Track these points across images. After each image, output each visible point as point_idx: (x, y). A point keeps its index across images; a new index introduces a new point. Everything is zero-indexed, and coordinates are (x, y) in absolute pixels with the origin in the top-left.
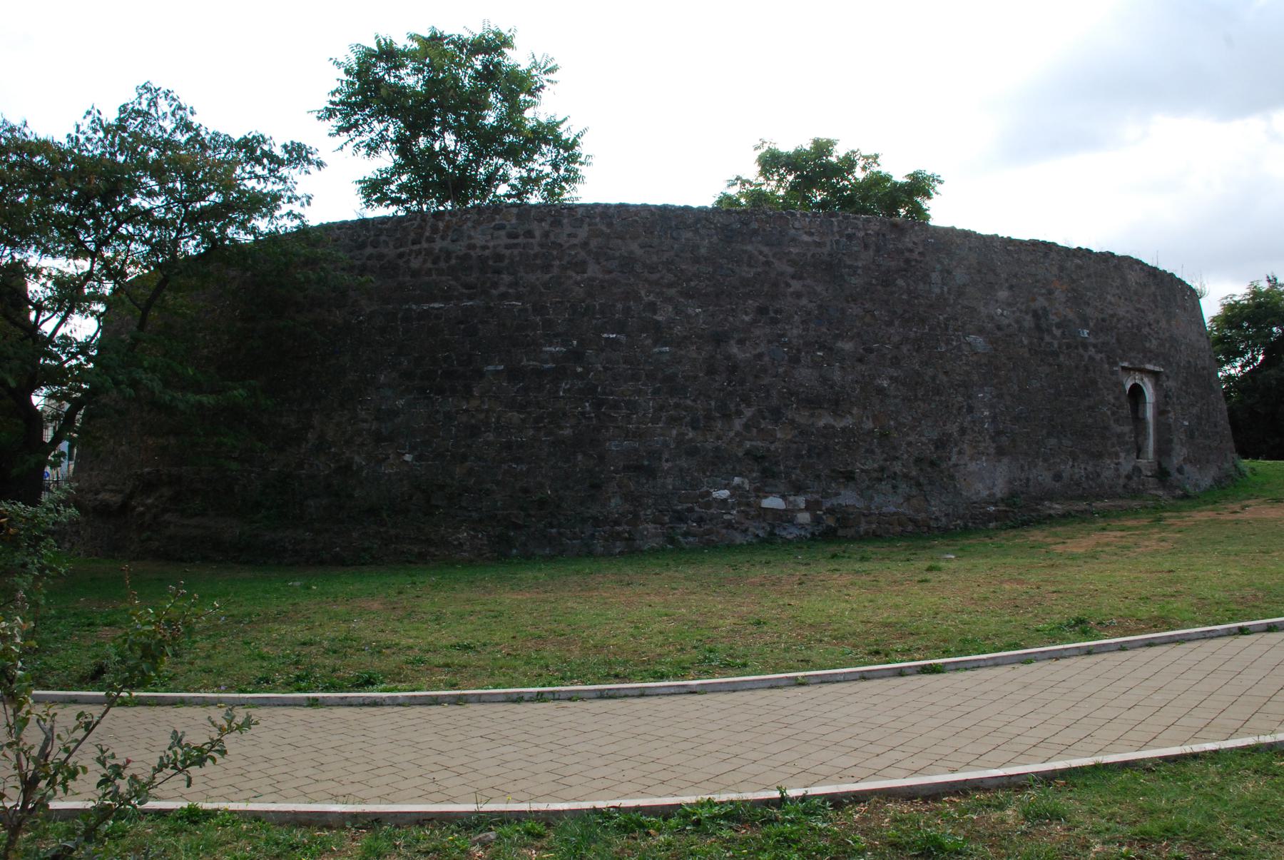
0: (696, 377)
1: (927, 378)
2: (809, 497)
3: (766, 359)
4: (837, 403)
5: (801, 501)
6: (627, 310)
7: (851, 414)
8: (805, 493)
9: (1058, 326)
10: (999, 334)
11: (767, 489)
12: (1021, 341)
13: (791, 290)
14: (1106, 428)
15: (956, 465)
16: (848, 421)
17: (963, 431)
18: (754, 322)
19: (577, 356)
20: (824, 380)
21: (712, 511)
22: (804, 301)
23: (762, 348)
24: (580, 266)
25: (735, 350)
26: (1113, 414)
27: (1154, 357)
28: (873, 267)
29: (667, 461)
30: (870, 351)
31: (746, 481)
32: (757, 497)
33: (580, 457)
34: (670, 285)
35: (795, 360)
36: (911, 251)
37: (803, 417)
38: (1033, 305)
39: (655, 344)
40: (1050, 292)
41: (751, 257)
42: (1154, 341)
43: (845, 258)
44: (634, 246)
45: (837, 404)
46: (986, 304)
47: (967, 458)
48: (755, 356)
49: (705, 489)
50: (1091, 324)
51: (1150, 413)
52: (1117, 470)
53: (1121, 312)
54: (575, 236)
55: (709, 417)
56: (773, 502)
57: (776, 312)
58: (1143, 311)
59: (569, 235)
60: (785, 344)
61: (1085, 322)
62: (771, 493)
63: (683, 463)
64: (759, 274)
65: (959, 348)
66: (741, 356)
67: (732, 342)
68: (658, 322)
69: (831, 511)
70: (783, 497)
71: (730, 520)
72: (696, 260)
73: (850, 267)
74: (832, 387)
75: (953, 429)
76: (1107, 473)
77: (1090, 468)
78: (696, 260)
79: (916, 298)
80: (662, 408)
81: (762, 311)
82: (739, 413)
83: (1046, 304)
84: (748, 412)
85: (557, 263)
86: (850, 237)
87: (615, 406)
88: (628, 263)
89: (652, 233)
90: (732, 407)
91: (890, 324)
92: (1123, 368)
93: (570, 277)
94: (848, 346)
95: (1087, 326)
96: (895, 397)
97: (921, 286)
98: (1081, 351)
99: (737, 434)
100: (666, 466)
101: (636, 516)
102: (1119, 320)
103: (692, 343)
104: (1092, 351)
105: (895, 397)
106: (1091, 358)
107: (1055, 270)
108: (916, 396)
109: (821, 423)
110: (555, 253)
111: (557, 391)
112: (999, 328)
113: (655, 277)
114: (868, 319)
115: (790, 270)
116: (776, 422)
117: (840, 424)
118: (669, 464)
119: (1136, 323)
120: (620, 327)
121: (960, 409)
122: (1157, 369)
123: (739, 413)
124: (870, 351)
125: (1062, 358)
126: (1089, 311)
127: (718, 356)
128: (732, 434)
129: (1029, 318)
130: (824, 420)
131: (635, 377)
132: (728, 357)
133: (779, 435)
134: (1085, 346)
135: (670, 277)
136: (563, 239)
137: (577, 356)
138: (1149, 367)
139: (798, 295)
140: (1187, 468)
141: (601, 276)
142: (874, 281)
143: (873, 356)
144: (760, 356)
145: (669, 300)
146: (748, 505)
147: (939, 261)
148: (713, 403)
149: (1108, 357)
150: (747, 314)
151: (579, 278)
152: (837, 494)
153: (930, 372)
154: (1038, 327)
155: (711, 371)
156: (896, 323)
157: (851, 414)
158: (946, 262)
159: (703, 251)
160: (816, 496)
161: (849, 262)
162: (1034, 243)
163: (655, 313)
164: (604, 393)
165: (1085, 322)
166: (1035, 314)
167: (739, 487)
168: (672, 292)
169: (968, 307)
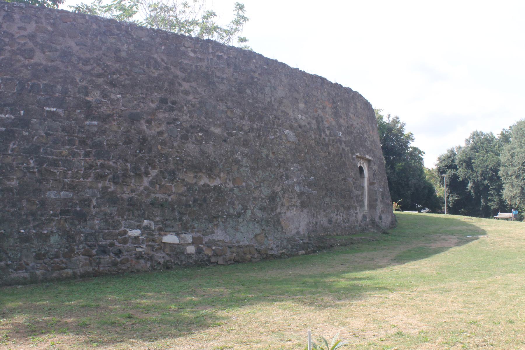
0: (116, 145)
1: (264, 156)
2: (194, 234)
3: (166, 135)
4: (211, 169)
5: (189, 237)
6: (65, 92)
7: (220, 177)
8: (192, 232)
9: (328, 128)
10: (300, 130)
11: (167, 229)
12: (311, 136)
13: (182, 88)
14: (350, 192)
15: (280, 213)
16: (217, 182)
17: (284, 191)
18: (159, 108)
19: (25, 123)
20: (202, 152)
21: (128, 245)
22: (191, 97)
23: (163, 128)
24: (30, 54)
25: (144, 127)
26: (354, 183)
27: (369, 152)
28: (232, 79)
29: (94, 207)
30: (231, 134)
31: (152, 223)
32: (160, 234)
33: (24, 203)
34: (99, 76)
35: (185, 138)
37: (189, 178)
38: (316, 114)
39: (87, 117)
40: (324, 108)
41: (156, 61)
43: (216, 71)
44: (72, 43)
45: (210, 171)
47: (285, 208)
48: (158, 133)
49: (123, 229)
50: (343, 129)
52: (356, 217)
54: (25, 29)
55: (125, 175)
56: (170, 239)
57: (174, 103)
59: (19, 28)
60: (177, 126)
61: (340, 126)
62: (170, 232)
63: (107, 209)
64: (162, 75)
65: (280, 137)
66: (148, 132)
67: (143, 122)
68: (89, 102)
69: (209, 245)
70: (178, 235)
71: (141, 252)
72: (118, 59)
73: (218, 77)
74: (207, 158)
75: (279, 189)
76: (353, 219)
77: (345, 217)
78: (118, 59)
79: (257, 102)
80: (91, 167)
81: (163, 101)
82: (147, 174)
84: (154, 173)
85: (8, 48)
86: (219, 58)
87: (55, 164)
88: (66, 55)
89: (86, 35)
90: (143, 169)
91: (242, 118)
92: (358, 157)
93: (18, 61)
94: (217, 131)
95: (340, 130)
96: (246, 167)
97: (260, 95)
98: (339, 144)
99: (146, 189)
100: (94, 211)
101: (72, 251)
103: (114, 120)
104: (343, 146)
105: (246, 167)
106: (343, 150)
107: (326, 94)
108: (258, 167)
109: (202, 183)
110: (7, 40)
111: (6, 150)
112: (300, 126)
113: (89, 68)
114: (229, 113)
115: (182, 75)
116: (172, 181)
117: (213, 183)
118: (97, 210)
120: (60, 103)
121: (281, 177)
122: (370, 158)
123: (147, 174)
124: (231, 134)
125: (330, 148)
126: (342, 121)
127: (133, 131)
128: (142, 188)
129: (314, 122)
130: (204, 180)
131: (71, 142)
132: (140, 132)
133: (174, 190)
134: (340, 141)
135: (98, 70)
136: (14, 29)
137: (25, 123)
138: (368, 157)
139: (187, 93)
140: (383, 217)
141: (44, 63)
142: (233, 89)
143: (232, 138)
144: (160, 133)
145: (97, 87)
146: (154, 241)
147: (269, 82)
148: (129, 165)
149: (351, 150)
150: (153, 102)
151: (27, 62)
152: (213, 232)
153: (265, 151)
154: (318, 128)
155: (128, 142)
156: (246, 118)
157: (220, 177)
158: (273, 81)
159: (123, 54)
160: (199, 234)
161: (218, 74)
162: (316, 77)
163: (87, 94)
164: (46, 153)
167: (147, 228)
168: (100, 80)
169: (284, 112)
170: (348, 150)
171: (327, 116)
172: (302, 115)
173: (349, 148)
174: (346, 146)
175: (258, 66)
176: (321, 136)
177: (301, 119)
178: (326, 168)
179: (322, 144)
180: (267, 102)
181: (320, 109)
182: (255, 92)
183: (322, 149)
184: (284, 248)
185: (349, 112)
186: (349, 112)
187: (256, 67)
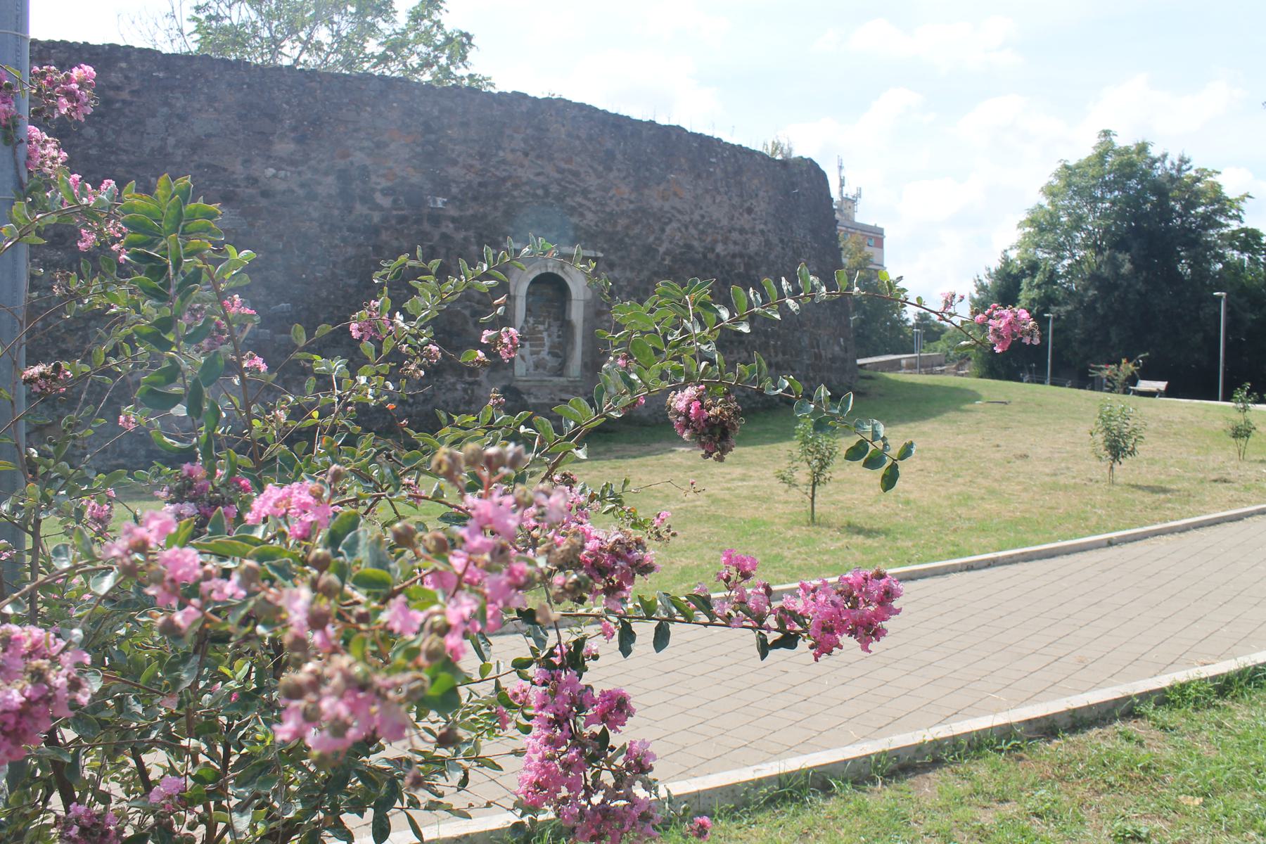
9: (386, 192)
36: (118, 88)
40: (379, 145)
42: (589, 215)
46: (247, 162)
50: (454, 190)
51: (577, 313)
53: (526, 174)
58: (576, 174)
79: (113, 153)
83: (368, 162)
98: (426, 226)
102: (516, 186)
106: (445, 237)
112: (265, 194)
119: (554, 189)
125: (385, 236)
126: (453, 171)
129: (331, 179)
134: (436, 218)
147: (166, 103)
165: (442, 186)
166: (343, 176)
169: (209, 166)
170: (466, 239)
171: (391, 164)
172: (279, 169)
173: (471, 233)
174: (457, 229)
175: (132, 75)
176: (350, 210)
177: (275, 176)
178: (353, 281)
179: (350, 229)
180: (147, 150)
181: (362, 149)
182: (110, 132)
183: (344, 239)
184: (121, 455)
185: (499, 147)
186: (499, 147)
187: (126, 77)
